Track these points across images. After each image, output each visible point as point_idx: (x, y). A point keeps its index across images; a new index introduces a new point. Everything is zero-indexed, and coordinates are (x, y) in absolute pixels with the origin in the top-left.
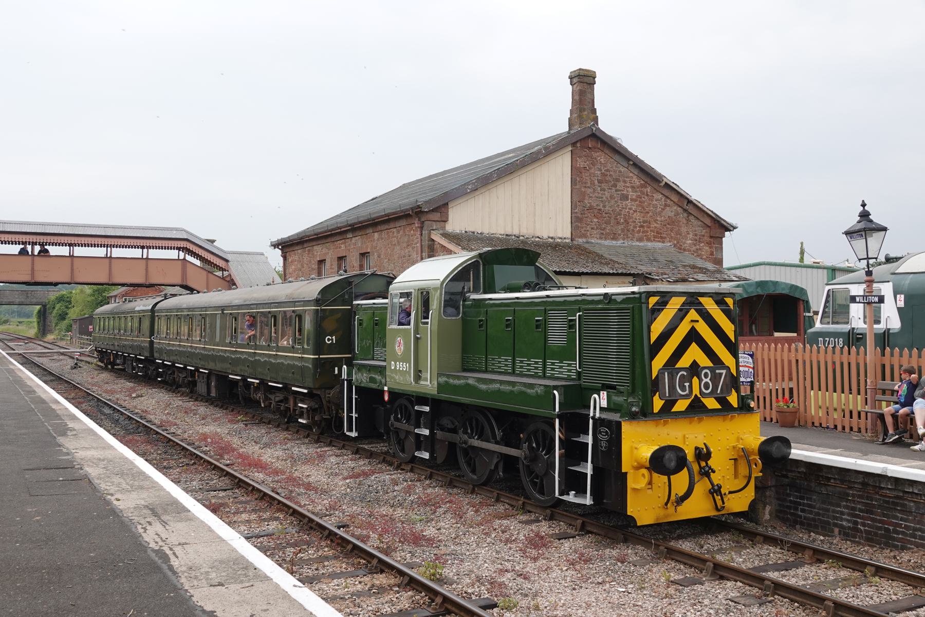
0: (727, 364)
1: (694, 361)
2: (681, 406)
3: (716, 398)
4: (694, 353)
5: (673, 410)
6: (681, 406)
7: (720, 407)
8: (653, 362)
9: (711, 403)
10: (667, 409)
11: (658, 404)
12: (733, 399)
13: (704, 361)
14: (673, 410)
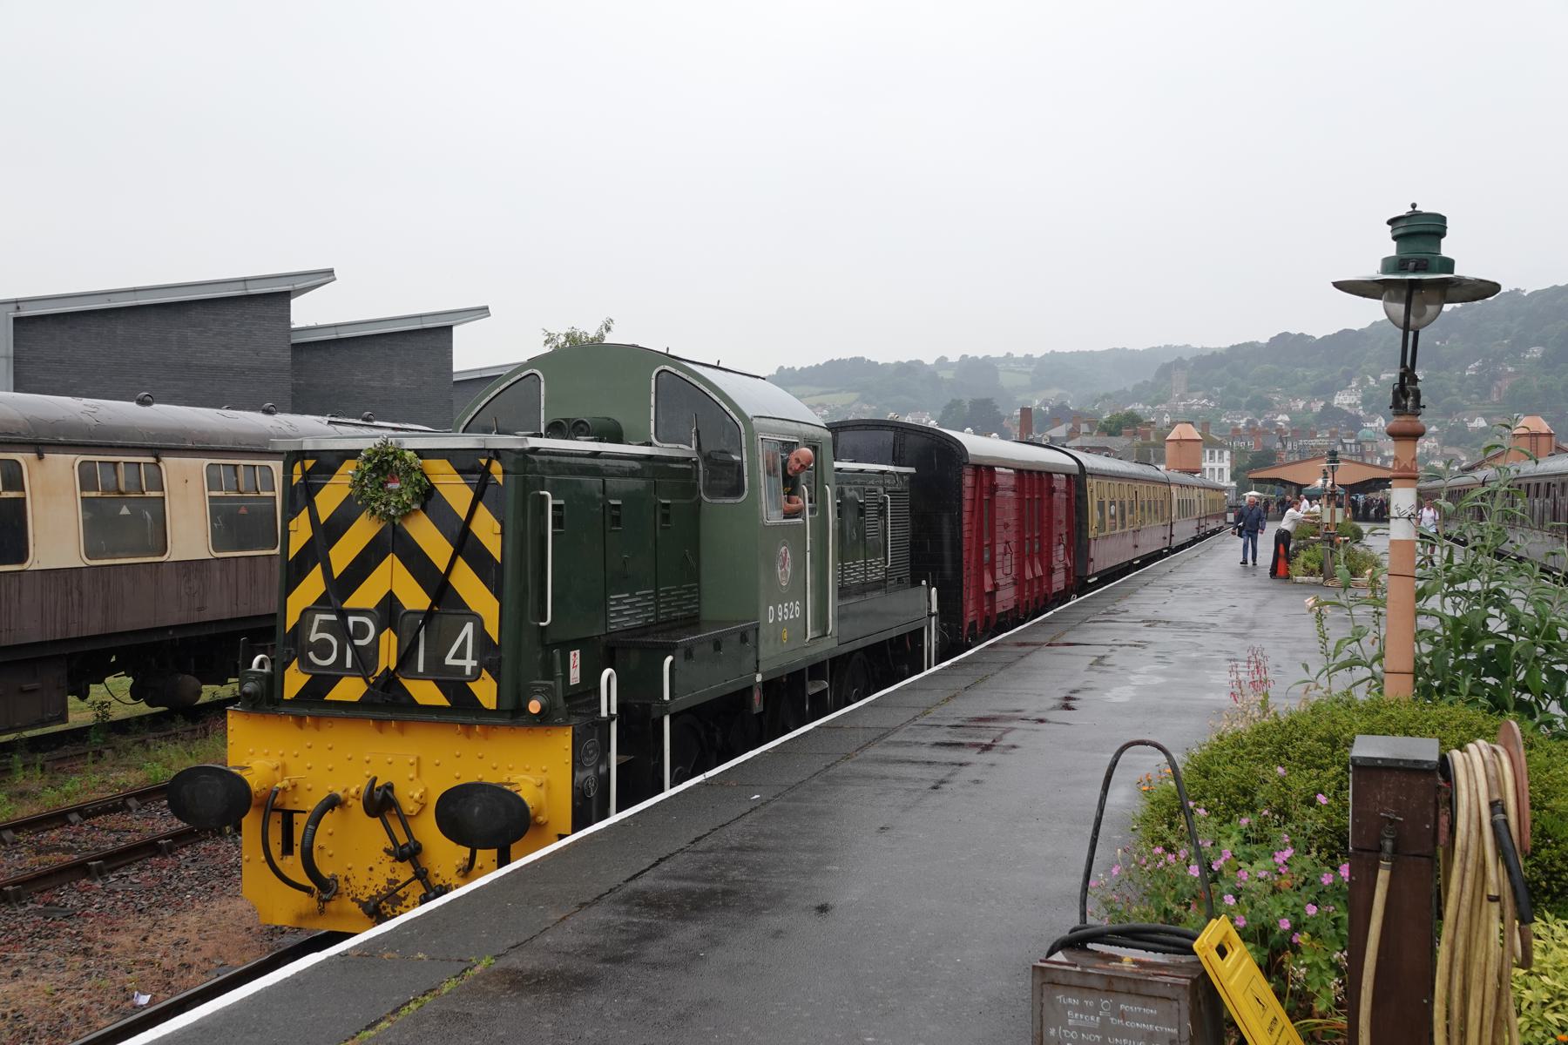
0: (474, 608)
1: (390, 594)
2: (350, 689)
3: (441, 685)
4: (393, 577)
5: (328, 697)
6: (350, 689)
7: (444, 702)
8: (289, 599)
9: (426, 692)
10: (315, 693)
11: (295, 681)
12: (486, 691)
13: (415, 598)
14: (328, 697)
